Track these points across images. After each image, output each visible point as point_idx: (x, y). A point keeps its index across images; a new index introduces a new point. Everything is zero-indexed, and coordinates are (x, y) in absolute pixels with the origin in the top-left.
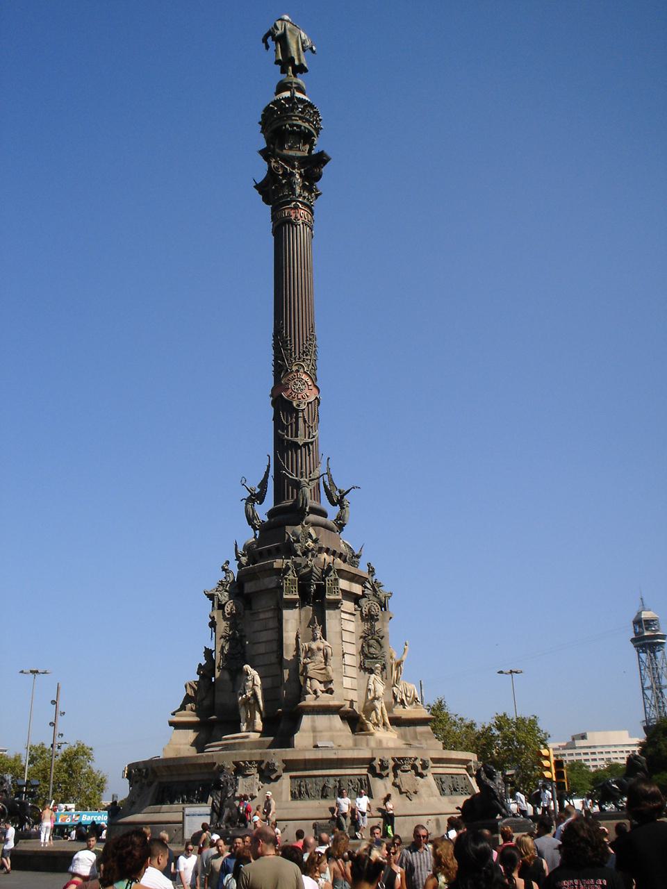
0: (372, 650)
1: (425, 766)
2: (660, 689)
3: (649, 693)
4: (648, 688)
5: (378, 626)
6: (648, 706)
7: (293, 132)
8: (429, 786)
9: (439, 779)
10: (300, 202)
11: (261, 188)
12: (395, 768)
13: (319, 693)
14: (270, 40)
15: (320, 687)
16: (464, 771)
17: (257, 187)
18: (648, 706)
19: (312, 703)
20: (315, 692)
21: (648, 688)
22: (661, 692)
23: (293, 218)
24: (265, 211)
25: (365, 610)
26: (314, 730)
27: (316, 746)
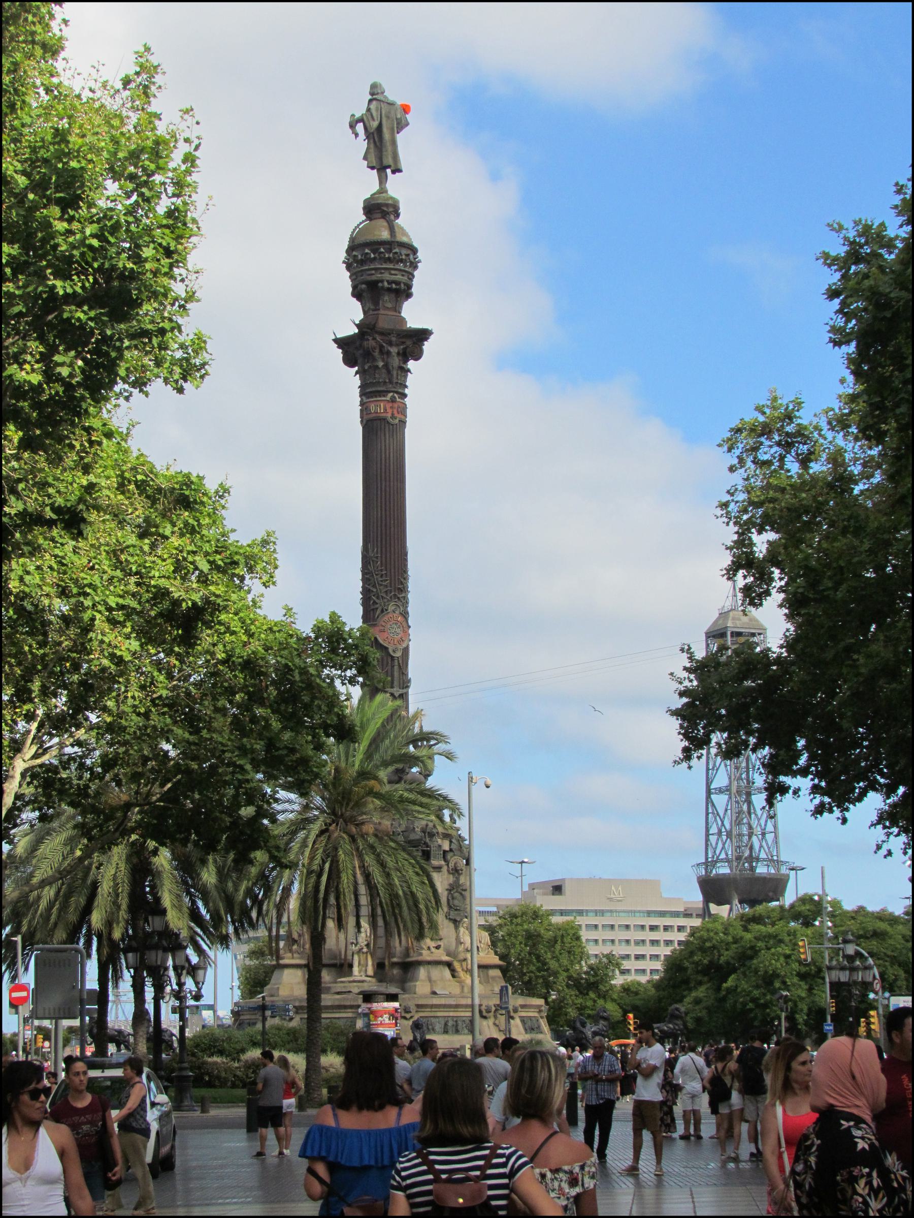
0: (456, 902)
1: (515, 1011)
2: (749, 794)
3: (720, 801)
4: (720, 791)
5: (462, 880)
6: (714, 830)
7: (389, 290)
8: (517, 1026)
9: (523, 1020)
10: (397, 393)
11: (342, 343)
12: (496, 1010)
13: (433, 950)
14: (360, 128)
15: (432, 944)
16: (536, 1014)
17: (336, 341)
18: (714, 830)
19: (429, 958)
20: (429, 948)
21: (720, 791)
22: (749, 803)
23: (389, 415)
24: (350, 380)
25: (451, 865)
26: (430, 980)
27: (434, 993)
